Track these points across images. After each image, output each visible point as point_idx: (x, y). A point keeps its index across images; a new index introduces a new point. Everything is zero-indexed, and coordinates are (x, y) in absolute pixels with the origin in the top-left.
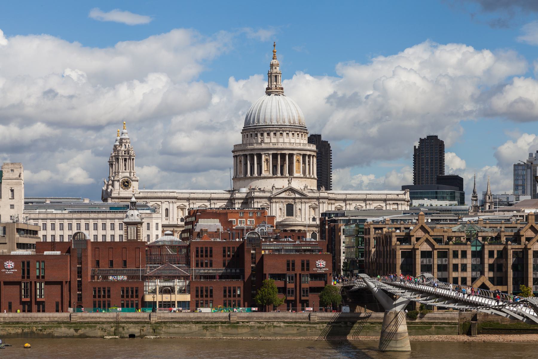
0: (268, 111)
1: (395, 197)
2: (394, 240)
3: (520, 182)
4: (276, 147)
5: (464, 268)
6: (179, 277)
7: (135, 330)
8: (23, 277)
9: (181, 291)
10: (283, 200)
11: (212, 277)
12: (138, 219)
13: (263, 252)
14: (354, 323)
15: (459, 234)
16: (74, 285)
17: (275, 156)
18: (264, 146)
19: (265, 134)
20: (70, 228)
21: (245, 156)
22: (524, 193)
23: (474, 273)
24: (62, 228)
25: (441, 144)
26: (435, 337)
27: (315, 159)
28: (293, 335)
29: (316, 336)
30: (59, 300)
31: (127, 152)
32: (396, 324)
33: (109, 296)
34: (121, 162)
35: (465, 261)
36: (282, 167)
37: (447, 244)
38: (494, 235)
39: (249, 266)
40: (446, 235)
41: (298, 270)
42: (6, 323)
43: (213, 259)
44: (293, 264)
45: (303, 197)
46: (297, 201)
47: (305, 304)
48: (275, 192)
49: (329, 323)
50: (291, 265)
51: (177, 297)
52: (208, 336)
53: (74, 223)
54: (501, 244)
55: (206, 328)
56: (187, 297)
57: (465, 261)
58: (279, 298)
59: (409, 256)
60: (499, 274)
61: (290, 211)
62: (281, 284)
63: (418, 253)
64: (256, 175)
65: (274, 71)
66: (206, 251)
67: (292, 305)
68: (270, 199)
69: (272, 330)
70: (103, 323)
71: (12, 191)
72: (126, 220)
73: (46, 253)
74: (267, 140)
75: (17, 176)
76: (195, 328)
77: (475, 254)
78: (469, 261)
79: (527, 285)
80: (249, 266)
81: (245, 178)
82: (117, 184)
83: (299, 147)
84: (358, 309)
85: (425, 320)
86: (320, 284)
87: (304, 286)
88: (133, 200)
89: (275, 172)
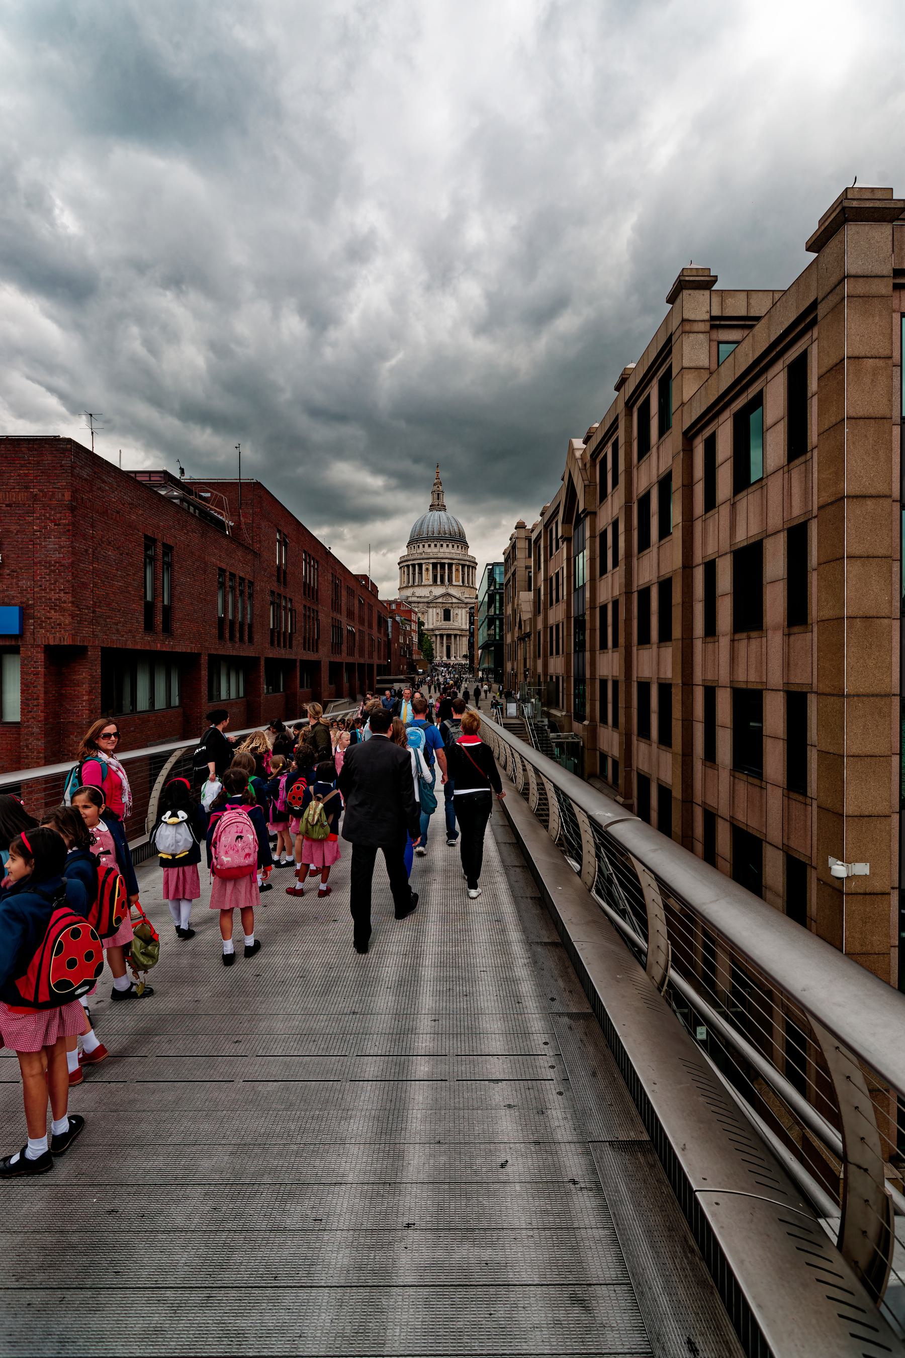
10: (441, 605)
17: (435, 565)
18: (424, 556)
19: (426, 545)
21: (408, 566)
45: (462, 603)
46: (454, 605)
61: (447, 616)
68: (428, 603)
81: (407, 587)
83: (458, 557)
89: (435, 580)
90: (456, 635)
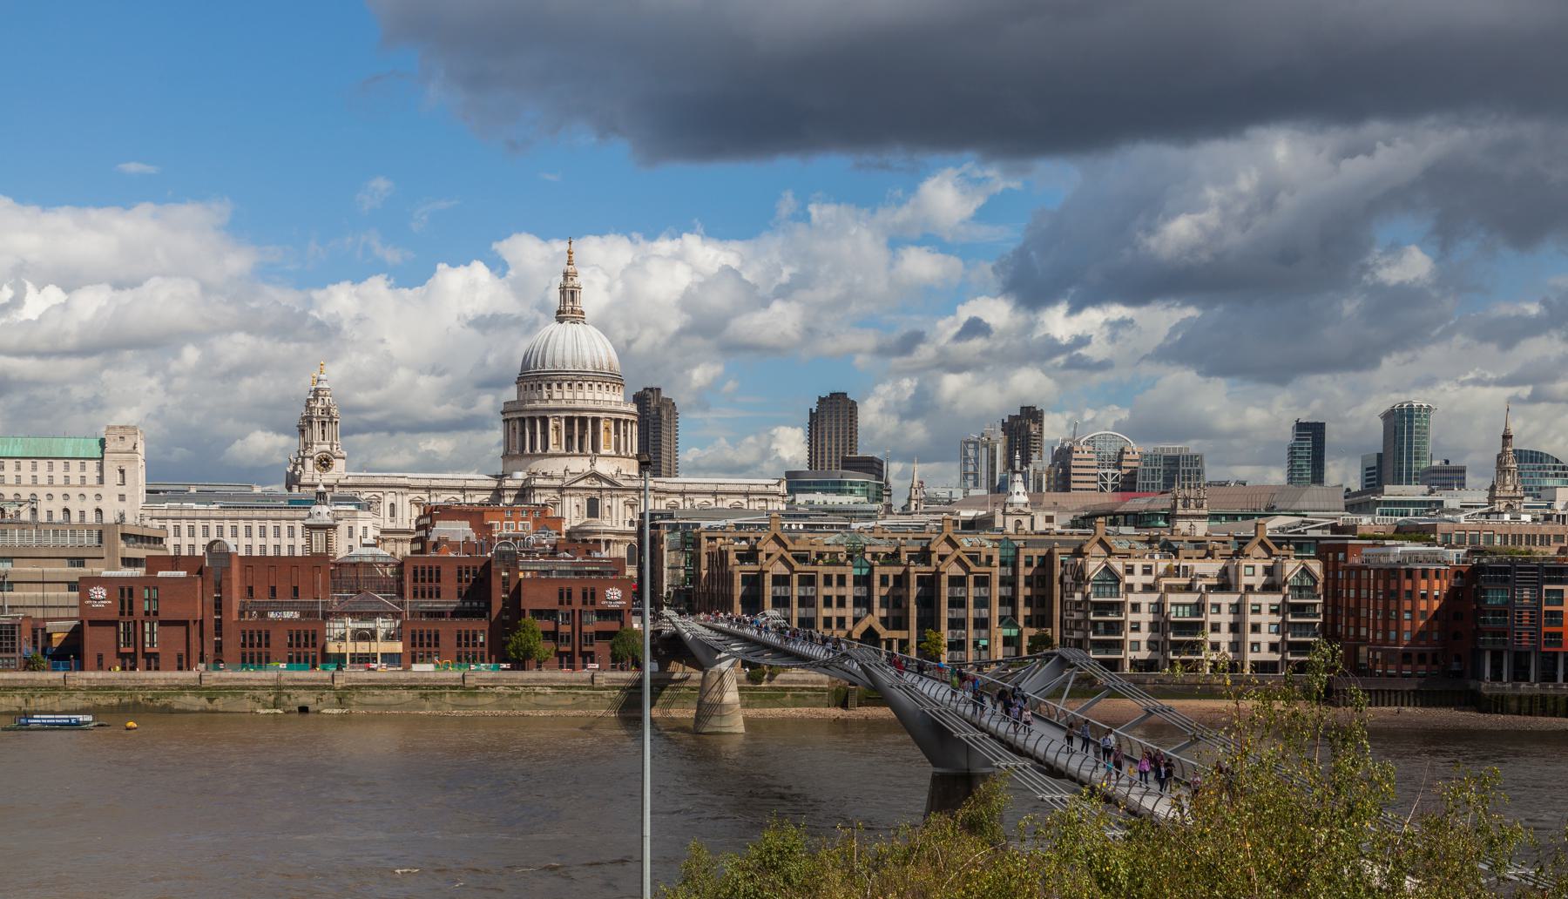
0: (559, 348)
1: (764, 488)
2: (732, 557)
3: (971, 469)
4: (571, 406)
5: (841, 602)
6: (384, 615)
7: (307, 699)
8: (122, 613)
9: (389, 637)
11: (441, 614)
12: (328, 520)
13: (521, 575)
14: (663, 688)
15: (836, 549)
16: (210, 626)
17: (570, 421)
18: (551, 404)
19: (554, 386)
20: (206, 533)
21: (522, 420)
22: (976, 485)
23: (858, 610)
24: (192, 534)
25: (852, 408)
26: (792, 711)
27: (635, 428)
28: (566, 707)
29: (604, 711)
30: (183, 650)
31: (327, 410)
32: (721, 690)
33: (267, 645)
34: (317, 427)
35: (842, 591)
36: (581, 438)
37: (814, 564)
38: (891, 550)
39: (498, 597)
40: (814, 550)
41: (577, 604)
42: (91, 688)
43: (442, 585)
44: (569, 595)
45: (614, 487)
47: (588, 657)
48: (568, 478)
49: (623, 689)
50: (565, 596)
51: (380, 647)
52: (428, 709)
53: (213, 525)
54: (899, 564)
55: (425, 696)
56: (398, 647)
57: (842, 591)
58: (545, 648)
59: (754, 583)
60: (896, 613)
61: (593, 509)
62: (549, 625)
63: (768, 579)
64: (539, 450)
65: (570, 283)
66: (430, 573)
67: (566, 660)
68: (560, 489)
69: (533, 699)
70: (255, 688)
71: (122, 472)
72: (308, 522)
73: (160, 574)
74: (557, 395)
75: (130, 448)
76: (407, 696)
77: (858, 581)
78: (849, 591)
79: (938, 630)
80: (498, 597)
82: (309, 463)
83: (609, 407)
84: (673, 666)
85: (775, 684)
86: (612, 625)
87: (587, 629)
88: (321, 488)
89: (569, 447)
90: (608, 542)
